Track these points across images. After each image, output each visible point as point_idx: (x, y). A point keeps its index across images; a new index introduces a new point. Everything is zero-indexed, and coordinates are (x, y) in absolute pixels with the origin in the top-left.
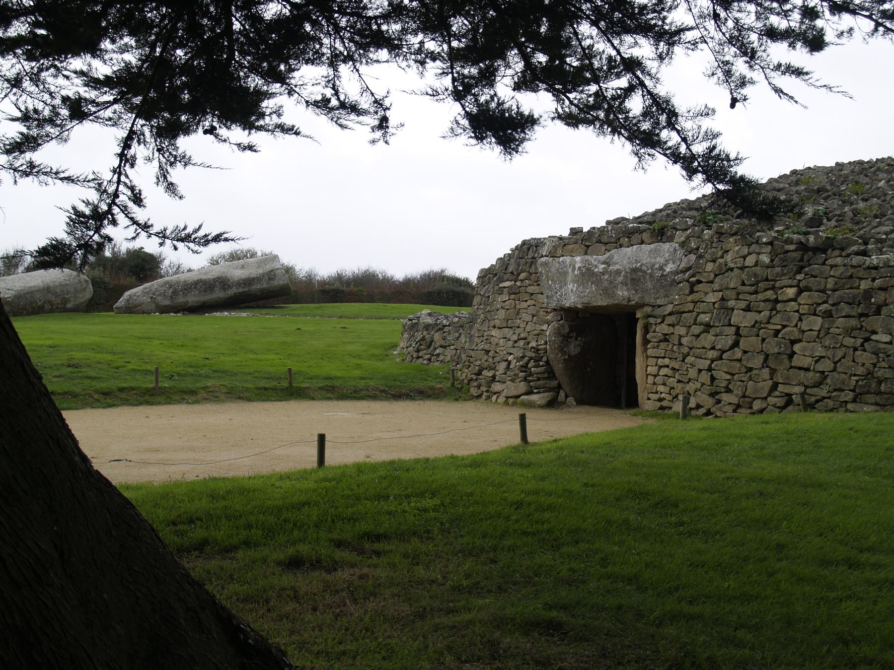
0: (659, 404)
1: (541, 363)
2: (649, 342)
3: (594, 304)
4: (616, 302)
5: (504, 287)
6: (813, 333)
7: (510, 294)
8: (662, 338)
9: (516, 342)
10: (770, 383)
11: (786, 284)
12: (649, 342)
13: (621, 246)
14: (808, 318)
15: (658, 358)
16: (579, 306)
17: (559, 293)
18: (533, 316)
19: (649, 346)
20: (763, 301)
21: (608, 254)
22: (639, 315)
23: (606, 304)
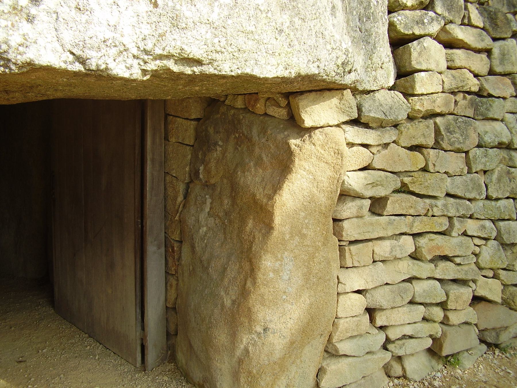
4: (313, 70)
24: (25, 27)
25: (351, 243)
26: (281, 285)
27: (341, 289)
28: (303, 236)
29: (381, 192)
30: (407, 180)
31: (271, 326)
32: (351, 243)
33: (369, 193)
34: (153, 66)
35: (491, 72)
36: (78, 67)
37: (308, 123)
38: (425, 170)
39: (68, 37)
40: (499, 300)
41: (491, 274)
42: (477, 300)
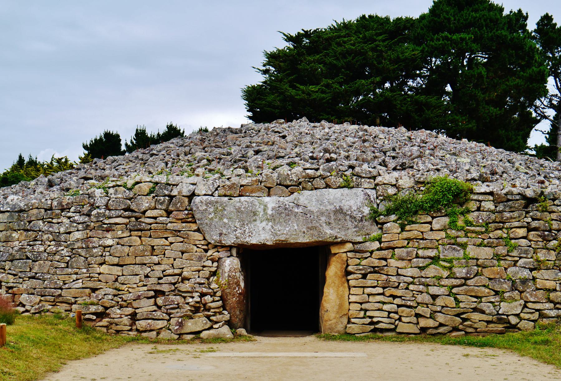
0: (372, 327)
1: (217, 299)
2: (350, 273)
3: (292, 241)
5: (116, 224)
6: (550, 262)
7: (131, 231)
8: (372, 270)
9: (160, 278)
10: (522, 302)
11: (517, 225)
12: (350, 273)
13: (304, 189)
14: (541, 251)
15: (364, 287)
16: (268, 243)
17: (239, 231)
18: (183, 253)
19: (349, 277)
20: (496, 239)
21: (293, 196)
22: (334, 250)
23: (308, 241)
24: (250, 238)
25: (355, 287)
26: (330, 297)
27: (350, 301)
28: (335, 283)
29: (363, 272)
30: (376, 269)
31: (328, 309)
32: (355, 287)
33: (359, 272)
34: (274, 243)
35: (432, 230)
36: (260, 243)
37: (333, 252)
38: (386, 266)
39: (257, 239)
40: (428, 316)
41: (425, 306)
42: (418, 316)
